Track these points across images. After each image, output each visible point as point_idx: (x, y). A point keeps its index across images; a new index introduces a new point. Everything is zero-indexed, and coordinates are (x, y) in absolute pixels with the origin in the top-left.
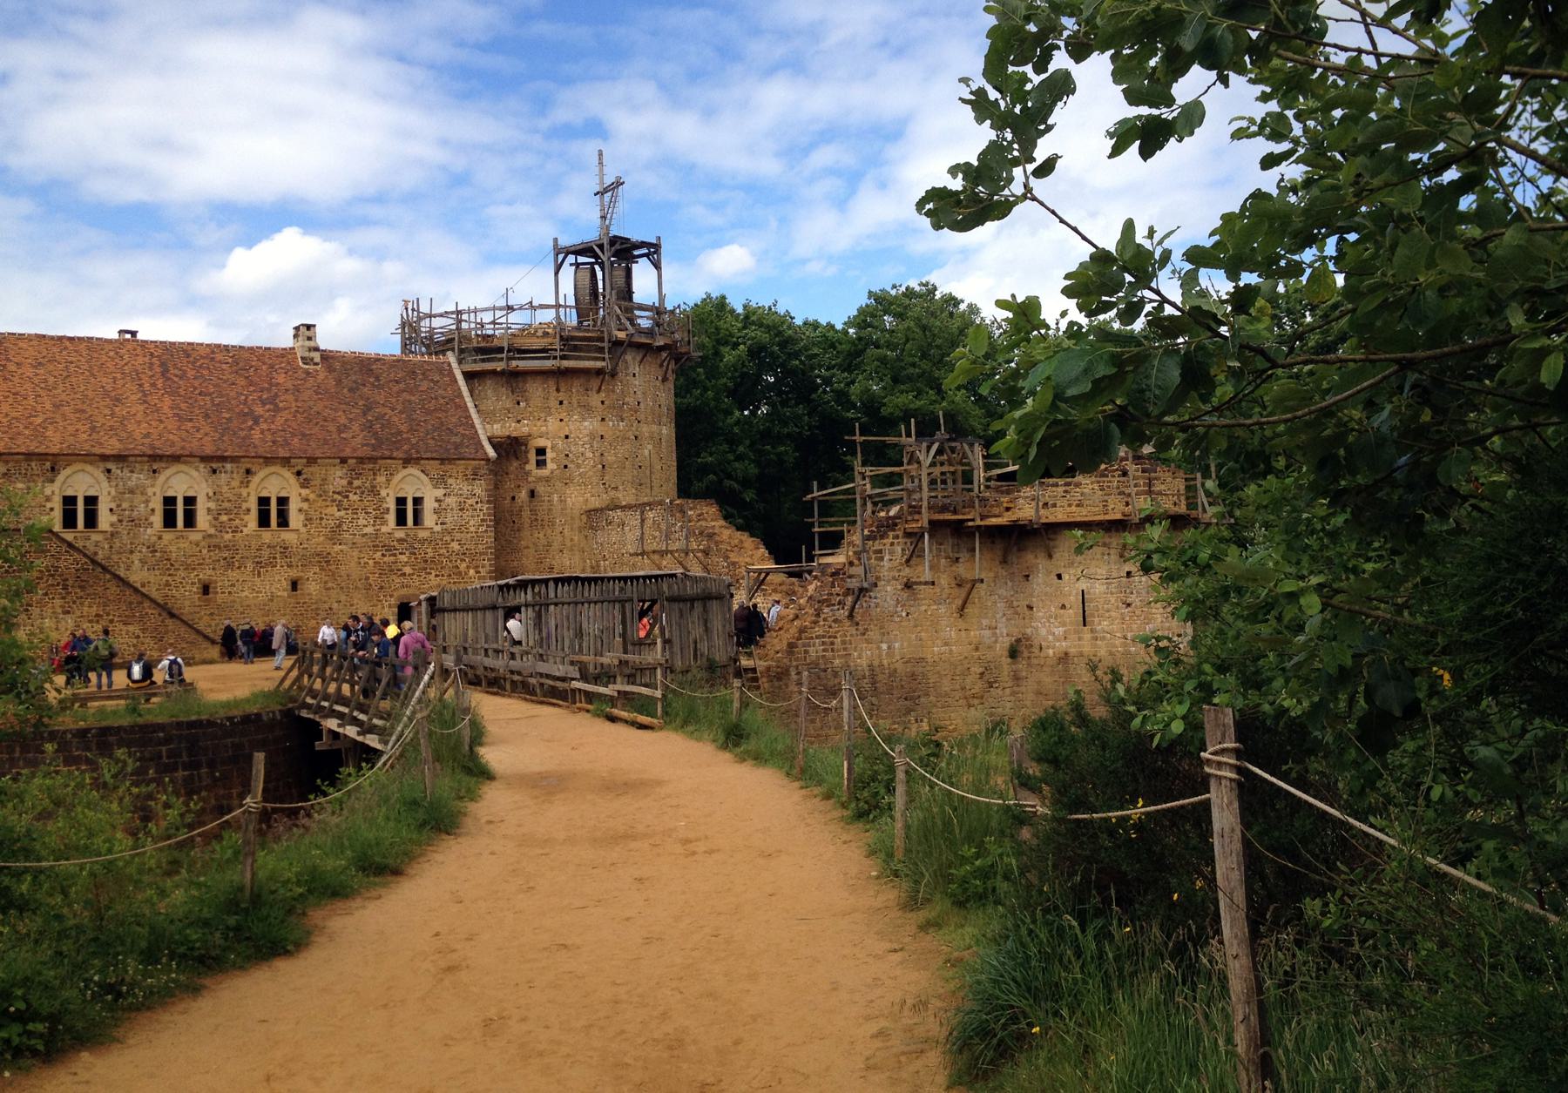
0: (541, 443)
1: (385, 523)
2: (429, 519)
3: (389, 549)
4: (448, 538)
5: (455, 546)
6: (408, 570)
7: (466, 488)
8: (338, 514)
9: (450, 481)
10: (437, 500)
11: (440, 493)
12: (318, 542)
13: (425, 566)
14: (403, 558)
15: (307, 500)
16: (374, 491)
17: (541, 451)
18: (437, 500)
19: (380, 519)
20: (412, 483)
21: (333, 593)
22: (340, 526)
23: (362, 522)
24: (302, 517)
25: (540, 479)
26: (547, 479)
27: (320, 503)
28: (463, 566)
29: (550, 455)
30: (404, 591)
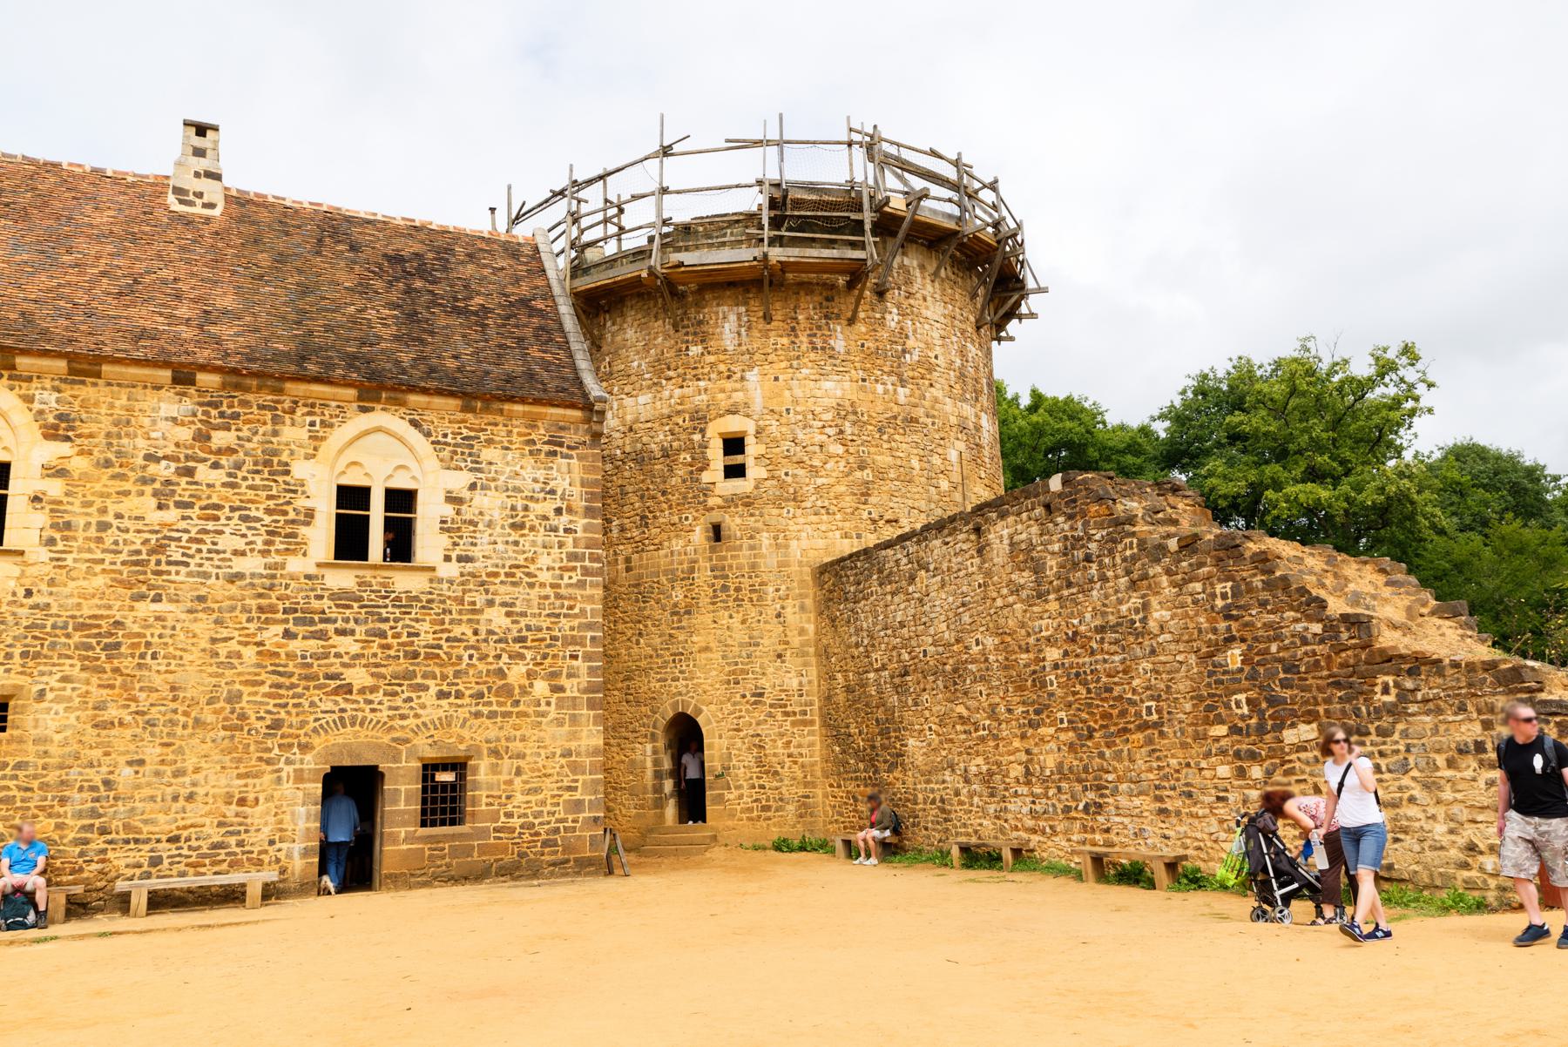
0: (733, 425)
1: (295, 546)
2: (428, 543)
3: (304, 618)
4: (480, 599)
5: (496, 618)
6: (358, 677)
7: (529, 473)
8: (155, 517)
9: (487, 454)
10: (452, 499)
11: (459, 481)
12: (87, 589)
13: (410, 668)
14: (348, 645)
15: (61, 473)
16: (273, 465)
17: (734, 445)
18: (452, 499)
19: (286, 535)
20: (382, 447)
21: (120, 739)
22: (160, 549)
23: (228, 542)
24: (41, 518)
25: (730, 502)
26: (748, 502)
27: (103, 482)
28: (516, 673)
29: (752, 448)
30: (346, 736)
